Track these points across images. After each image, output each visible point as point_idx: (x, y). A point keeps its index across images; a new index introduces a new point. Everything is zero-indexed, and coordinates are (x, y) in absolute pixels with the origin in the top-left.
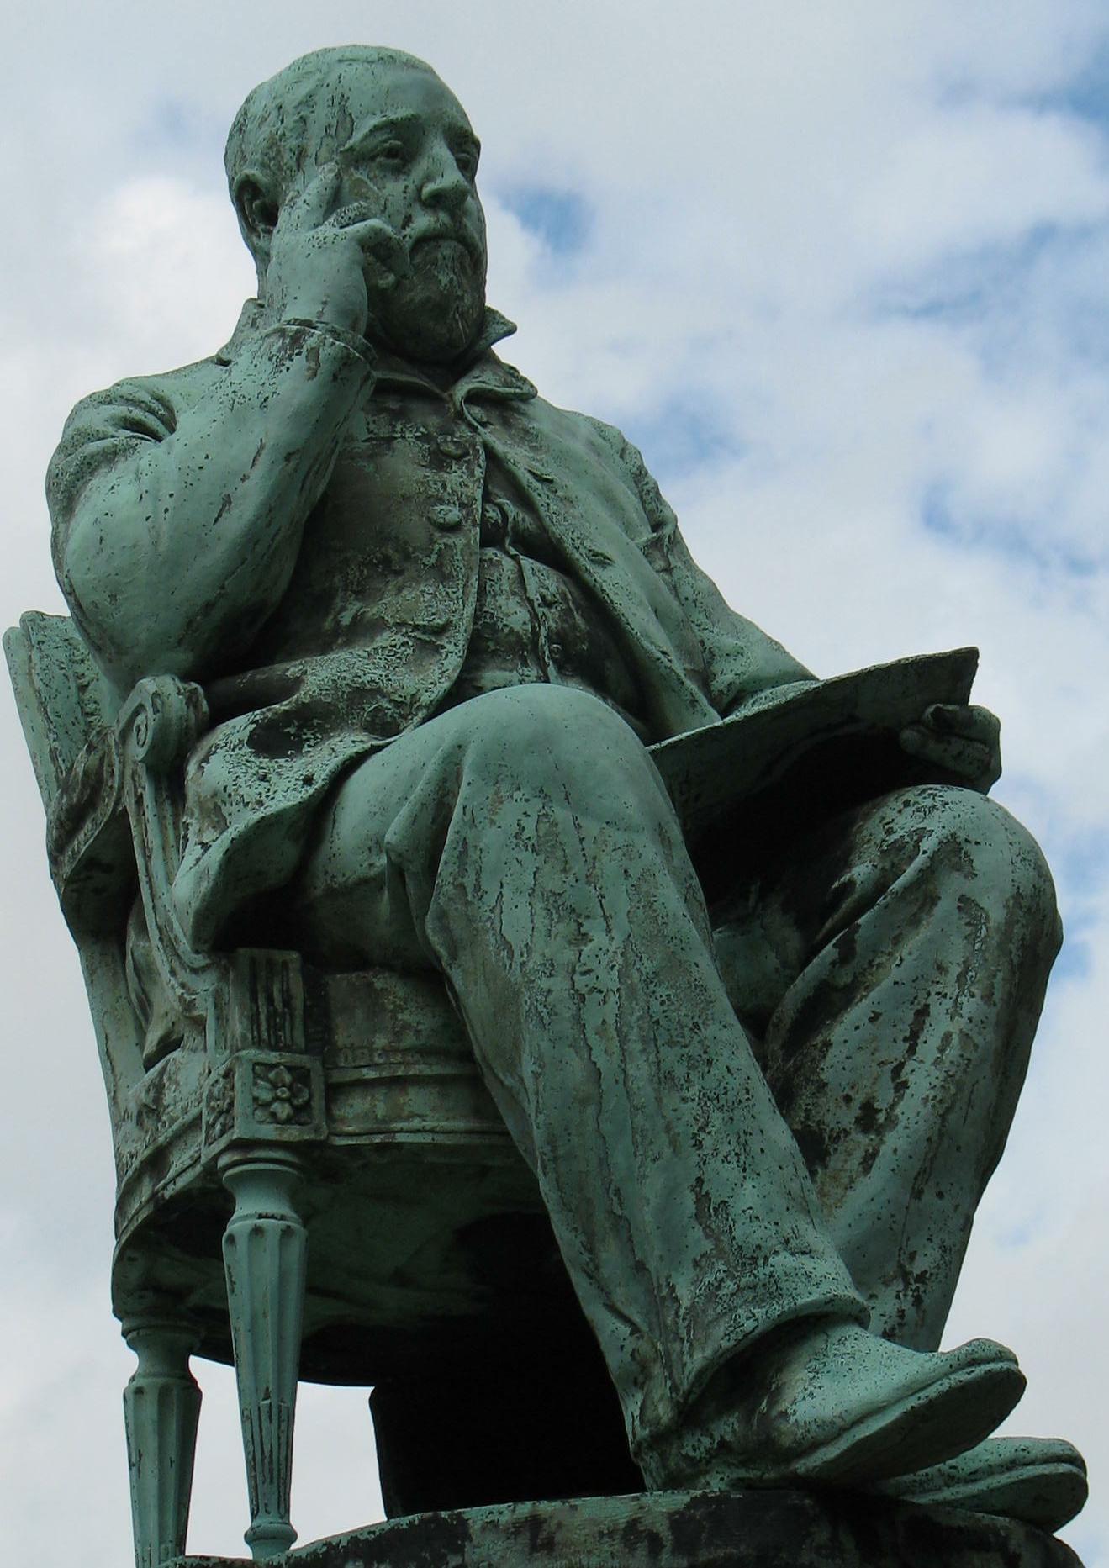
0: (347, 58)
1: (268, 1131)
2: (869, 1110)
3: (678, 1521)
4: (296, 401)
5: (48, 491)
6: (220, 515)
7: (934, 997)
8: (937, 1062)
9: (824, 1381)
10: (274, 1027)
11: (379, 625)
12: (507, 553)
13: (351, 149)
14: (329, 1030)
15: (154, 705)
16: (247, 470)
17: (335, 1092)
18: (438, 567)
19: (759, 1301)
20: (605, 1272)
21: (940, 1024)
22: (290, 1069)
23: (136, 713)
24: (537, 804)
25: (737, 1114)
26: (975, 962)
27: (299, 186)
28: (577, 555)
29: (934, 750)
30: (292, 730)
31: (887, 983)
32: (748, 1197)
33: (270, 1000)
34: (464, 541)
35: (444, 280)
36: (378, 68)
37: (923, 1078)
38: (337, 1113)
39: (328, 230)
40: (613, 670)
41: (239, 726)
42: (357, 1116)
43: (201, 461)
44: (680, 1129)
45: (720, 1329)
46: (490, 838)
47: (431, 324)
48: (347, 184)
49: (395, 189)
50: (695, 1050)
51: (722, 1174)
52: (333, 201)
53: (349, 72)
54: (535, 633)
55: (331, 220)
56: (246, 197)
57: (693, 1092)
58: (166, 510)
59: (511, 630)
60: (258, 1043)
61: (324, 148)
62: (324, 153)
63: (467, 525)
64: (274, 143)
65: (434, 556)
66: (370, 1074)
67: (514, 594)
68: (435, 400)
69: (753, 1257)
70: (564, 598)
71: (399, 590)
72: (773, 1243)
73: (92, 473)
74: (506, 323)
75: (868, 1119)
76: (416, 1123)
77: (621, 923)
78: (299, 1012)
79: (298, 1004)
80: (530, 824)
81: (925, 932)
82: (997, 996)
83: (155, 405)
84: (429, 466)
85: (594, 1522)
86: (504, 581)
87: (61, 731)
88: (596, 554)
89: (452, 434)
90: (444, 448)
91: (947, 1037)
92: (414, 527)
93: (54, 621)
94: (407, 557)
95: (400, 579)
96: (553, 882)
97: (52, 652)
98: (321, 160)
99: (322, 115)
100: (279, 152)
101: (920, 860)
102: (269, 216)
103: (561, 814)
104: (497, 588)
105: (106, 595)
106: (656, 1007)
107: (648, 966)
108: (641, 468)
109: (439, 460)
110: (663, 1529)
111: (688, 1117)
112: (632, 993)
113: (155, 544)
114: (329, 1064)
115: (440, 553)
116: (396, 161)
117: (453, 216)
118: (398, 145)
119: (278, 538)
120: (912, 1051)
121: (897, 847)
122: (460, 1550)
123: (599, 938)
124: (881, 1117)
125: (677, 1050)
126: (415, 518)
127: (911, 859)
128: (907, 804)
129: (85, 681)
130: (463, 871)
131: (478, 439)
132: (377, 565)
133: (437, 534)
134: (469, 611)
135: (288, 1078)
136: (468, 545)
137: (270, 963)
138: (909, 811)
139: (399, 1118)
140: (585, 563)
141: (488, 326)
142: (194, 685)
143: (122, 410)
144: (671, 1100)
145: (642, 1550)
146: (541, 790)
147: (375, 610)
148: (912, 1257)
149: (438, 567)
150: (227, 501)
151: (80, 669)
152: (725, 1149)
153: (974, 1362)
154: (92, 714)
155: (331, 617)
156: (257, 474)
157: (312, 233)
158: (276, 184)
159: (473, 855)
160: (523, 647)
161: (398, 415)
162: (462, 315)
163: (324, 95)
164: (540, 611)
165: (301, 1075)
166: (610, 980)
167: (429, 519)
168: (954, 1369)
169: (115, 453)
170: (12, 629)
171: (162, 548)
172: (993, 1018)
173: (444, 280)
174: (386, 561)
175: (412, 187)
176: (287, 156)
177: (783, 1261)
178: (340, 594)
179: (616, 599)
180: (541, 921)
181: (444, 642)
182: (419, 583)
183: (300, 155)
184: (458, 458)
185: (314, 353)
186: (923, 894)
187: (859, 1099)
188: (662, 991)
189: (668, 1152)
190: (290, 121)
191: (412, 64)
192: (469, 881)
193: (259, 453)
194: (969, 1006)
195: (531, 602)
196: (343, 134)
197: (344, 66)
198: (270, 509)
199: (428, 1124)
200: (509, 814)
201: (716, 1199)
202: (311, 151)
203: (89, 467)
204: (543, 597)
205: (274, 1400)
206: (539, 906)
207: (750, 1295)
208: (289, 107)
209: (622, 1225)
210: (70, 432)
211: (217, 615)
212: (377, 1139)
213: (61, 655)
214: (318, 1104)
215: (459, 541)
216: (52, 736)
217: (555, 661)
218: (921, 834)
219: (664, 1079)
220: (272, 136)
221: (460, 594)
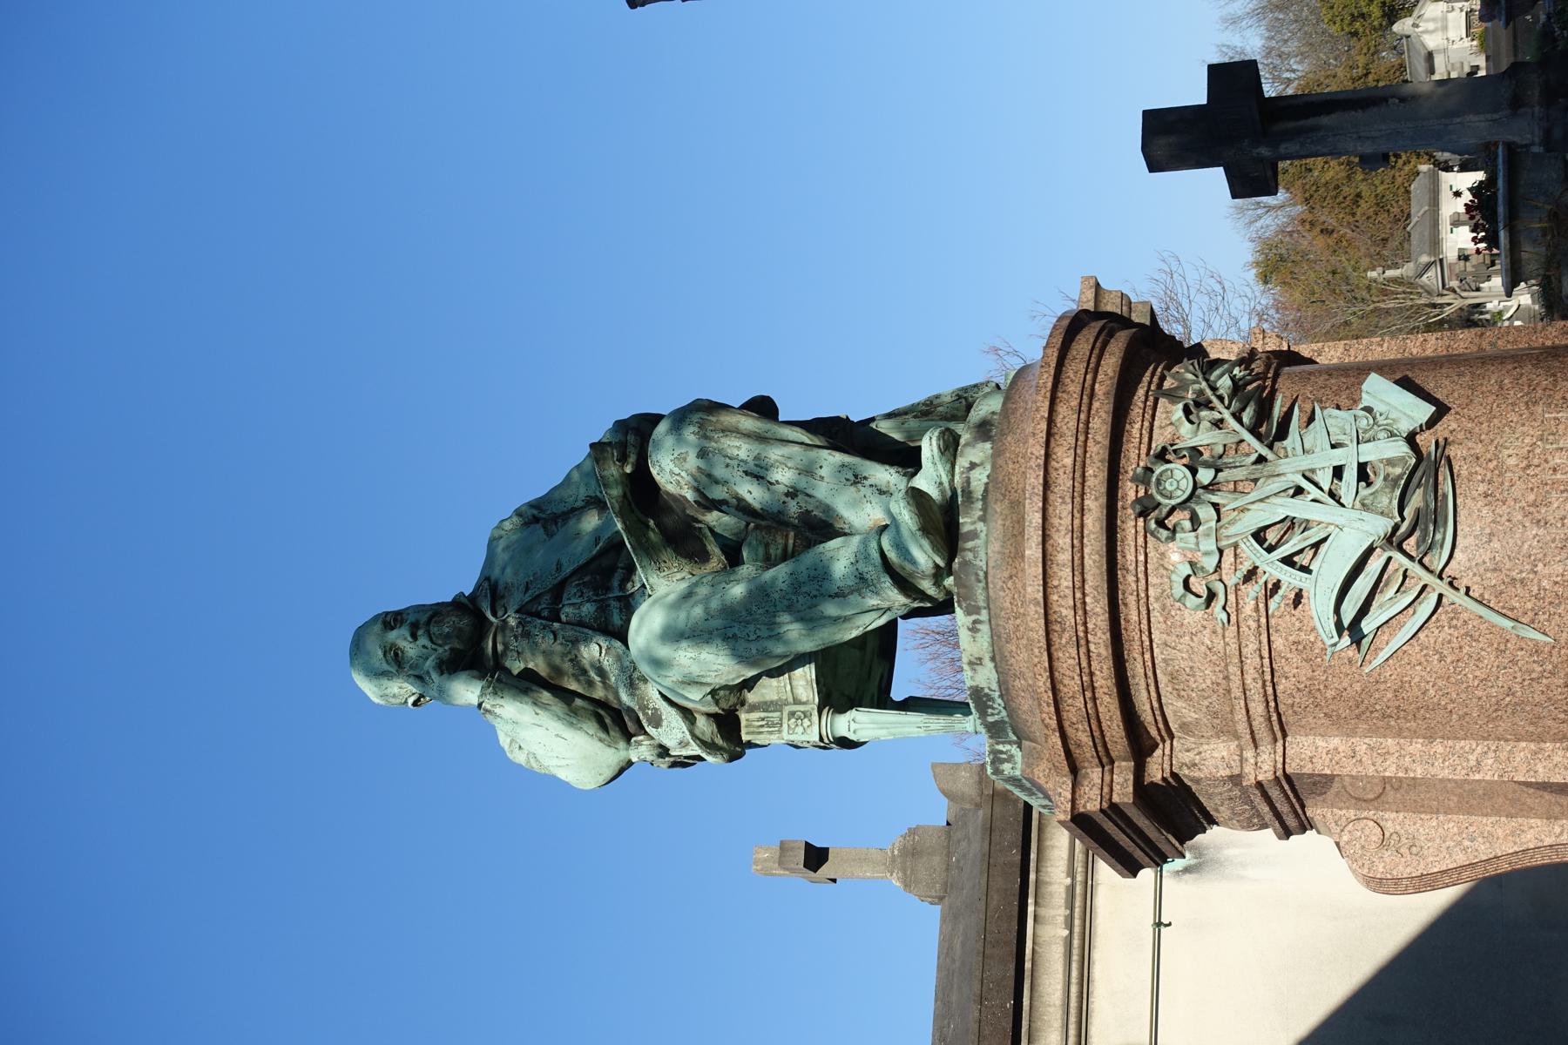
3: (968, 613)
10: (773, 725)
17: (797, 701)
79: (763, 715)
165: (792, 714)
187: (784, 498)
214: (802, 708)
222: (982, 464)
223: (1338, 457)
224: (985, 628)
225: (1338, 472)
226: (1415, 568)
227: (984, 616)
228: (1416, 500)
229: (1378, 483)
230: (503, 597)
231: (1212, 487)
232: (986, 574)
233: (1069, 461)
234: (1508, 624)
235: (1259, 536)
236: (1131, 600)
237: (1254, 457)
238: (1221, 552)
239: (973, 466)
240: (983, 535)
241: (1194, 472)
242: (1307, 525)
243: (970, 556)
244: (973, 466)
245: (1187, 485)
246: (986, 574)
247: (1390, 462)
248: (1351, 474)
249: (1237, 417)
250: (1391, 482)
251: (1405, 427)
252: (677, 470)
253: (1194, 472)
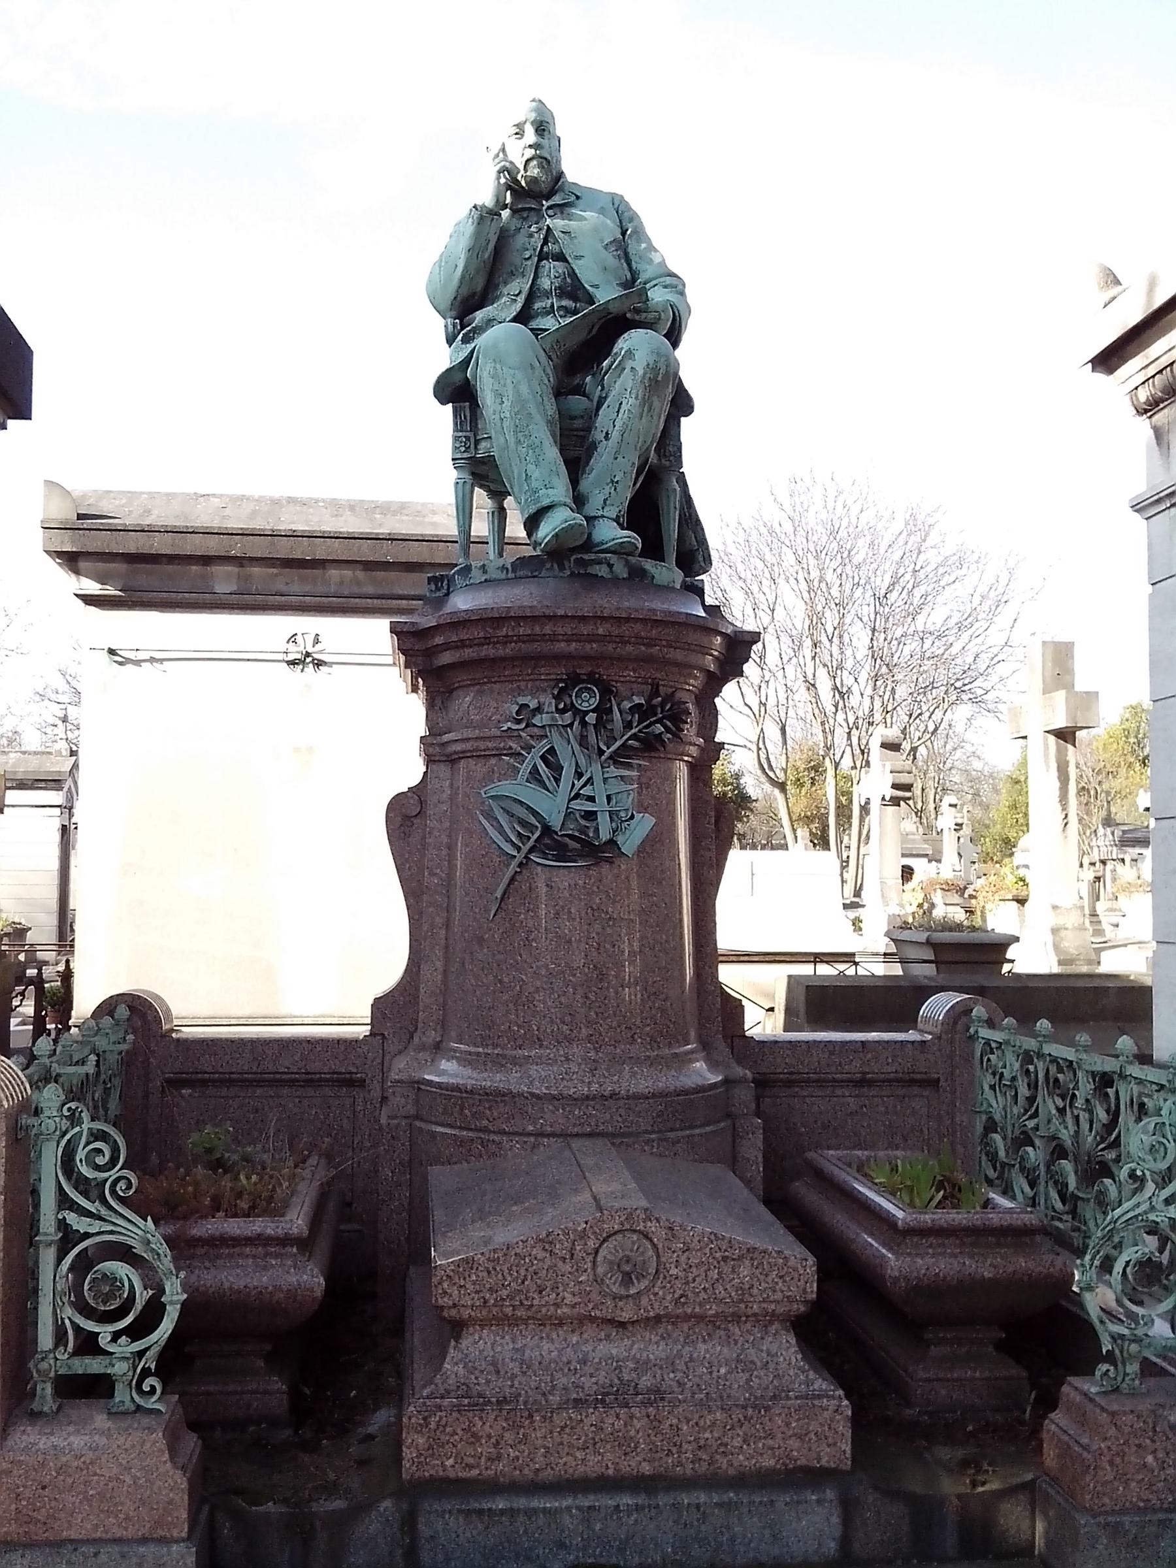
2: (607, 433)
17: (477, 442)
29: (637, 318)
37: (618, 423)
40: (580, 293)
46: (485, 374)
51: (531, 467)
75: (607, 437)
92: (517, 261)
103: (498, 366)
110: (509, 567)
156: (463, 256)
161: (525, 219)
165: (468, 438)
186: (621, 368)
198: (466, 267)
215: (529, 263)
222: (611, 571)
223: (601, 799)
225: (591, 799)
226: (531, 843)
227: (511, 575)
228: (573, 844)
229: (583, 822)
230: (562, 213)
231: (584, 724)
233: (600, 631)
234: (499, 894)
235: (552, 751)
236: (517, 671)
237: (605, 748)
238: (543, 727)
239: (610, 566)
241: (593, 711)
242: (557, 780)
243: (548, 566)
244: (610, 566)
245: (584, 707)
247: (597, 830)
248: (589, 807)
249: (634, 737)
250: (584, 830)
251: (620, 840)
253: (593, 711)
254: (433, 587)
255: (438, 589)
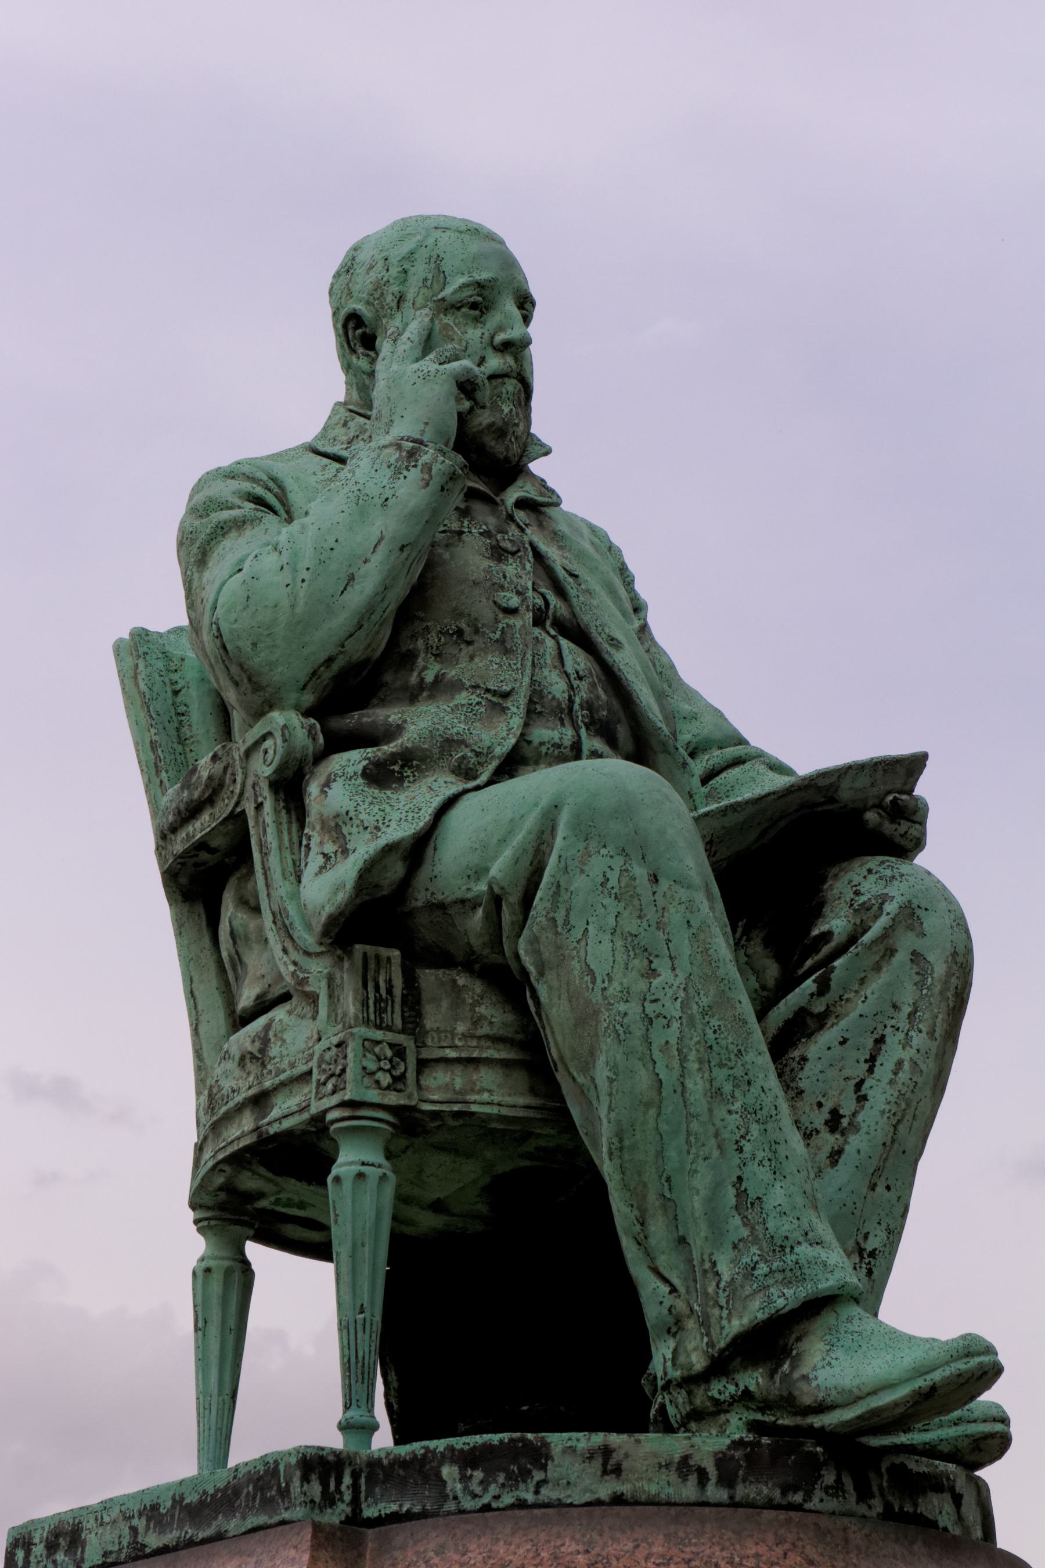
0: (442, 226)
1: (373, 1096)
3: (722, 1460)
4: (411, 504)
5: (180, 544)
6: (345, 589)
7: (889, 1030)
8: (891, 1082)
9: (839, 1353)
10: (380, 1011)
11: (457, 686)
12: (548, 633)
13: (443, 299)
14: (419, 1015)
15: (283, 735)
16: (369, 555)
17: (423, 1065)
18: (502, 641)
19: (788, 1283)
20: (652, 1241)
21: (893, 1052)
22: (391, 1046)
23: (264, 738)
24: (618, 862)
25: (770, 1126)
26: (923, 1005)
27: (397, 322)
28: (600, 639)
29: (888, 828)
30: (396, 768)
31: (854, 1015)
32: (777, 1196)
33: (377, 988)
34: (521, 623)
35: (506, 410)
36: (466, 237)
38: (422, 1082)
39: (429, 364)
40: (623, 732)
41: (354, 760)
42: (438, 1090)
43: (331, 543)
44: (725, 1135)
45: (756, 1304)
47: (493, 443)
48: (437, 326)
49: (474, 334)
50: (738, 1072)
51: (758, 1176)
52: (427, 344)
53: (445, 238)
54: (571, 701)
55: (432, 356)
56: (351, 325)
57: (737, 1106)
58: (303, 581)
59: (554, 698)
60: (367, 1022)
61: (421, 296)
62: (420, 301)
63: (522, 610)
64: (379, 286)
65: (499, 633)
66: (452, 1054)
67: (555, 667)
68: (490, 501)
69: (783, 1247)
70: (591, 673)
71: (472, 658)
72: (798, 1235)
73: (224, 535)
74: (542, 445)
76: (486, 1096)
77: (683, 962)
78: (398, 1000)
79: (398, 992)
80: (613, 877)
81: (885, 977)
82: (937, 1035)
83: (271, 484)
84: (492, 557)
85: (655, 1455)
86: (548, 656)
87: (160, 727)
88: (612, 639)
89: (506, 533)
90: (503, 544)
91: (900, 1063)
93: (155, 637)
94: (477, 631)
95: (471, 648)
96: (630, 924)
97: (154, 662)
98: (418, 305)
99: (420, 270)
100: (382, 294)
101: (883, 921)
102: (369, 342)
104: (542, 661)
105: (249, 643)
106: (709, 1032)
107: (705, 1001)
108: (623, 564)
109: (499, 554)
111: (732, 1126)
112: (692, 1023)
113: (293, 606)
114: (420, 1045)
115: (503, 630)
116: (477, 313)
117: (516, 360)
118: (478, 302)
119: (388, 611)
120: (871, 1071)
121: (866, 907)
122: (544, 1468)
123: (666, 974)
124: (845, 1122)
125: (725, 1071)
126: (484, 600)
127: (876, 917)
128: (870, 871)
129: (178, 687)
130: (555, 907)
131: (526, 539)
132: (452, 635)
133: (501, 615)
134: (526, 680)
135: (389, 1053)
136: (524, 626)
137: (378, 957)
138: (872, 878)
139: (472, 1090)
140: (605, 646)
141: (532, 447)
142: (312, 721)
143: (247, 486)
144: (720, 1112)
145: (693, 1479)
146: (623, 850)
147: (453, 673)
148: (866, 1237)
149: (502, 641)
150: (352, 578)
151: (175, 677)
152: (760, 1155)
153: (968, 1355)
154: (183, 715)
155: (415, 674)
156: (376, 559)
157: (416, 366)
158: (378, 318)
159: (565, 896)
160: (562, 711)
162: (516, 438)
163: (422, 254)
164: (575, 683)
165: (399, 1052)
166: (674, 1010)
167: (495, 602)
168: (953, 1359)
169: (244, 522)
170: (121, 640)
171: (299, 610)
172: (934, 1051)
173: (506, 410)
174: (460, 632)
175: (487, 335)
176: (389, 298)
177: (804, 1251)
178: (422, 655)
179: (629, 677)
180: (621, 957)
181: (509, 704)
182: (486, 653)
183: (400, 299)
184: (513, 554)
185: (428, 468)
187: (828, 1106)
188: (714, 1022)
189: (716, 1153)
190: (394, 271)
191: (491, 237)
192: (560, 916)
193: (379, 542)
194: (918, 1040)
195: (567, 675)
196: (436, 287)
197: (439, 231)
199: (496, 1098)
200: (597, 865)
201: (752, 1195)
202: (410, 296)
203: (222, 530)
204: (577, 673)
205: (367, 1315)
206: (619, 943)
207: (779, 1276)
208: (394, 260)
209: (670, 1205)
210: (200, 497)
211: (336, 667)
212: (456, 1108)
213: (160, 664)
214: (411, 1075)
215: (517, 622)
216: (153, 731)
217: (585, 724)
218: (884, 899)
219: (716, 1094)
220: (378, 281)
221: (519, 665)
224: (689, 1491)
232: (798, 1508)
240: (862, 1509)
243: (829, 1478)
246: (798, 1508)
252: (891, 907)
254: (315, 1489)
255: (329, 1500)
